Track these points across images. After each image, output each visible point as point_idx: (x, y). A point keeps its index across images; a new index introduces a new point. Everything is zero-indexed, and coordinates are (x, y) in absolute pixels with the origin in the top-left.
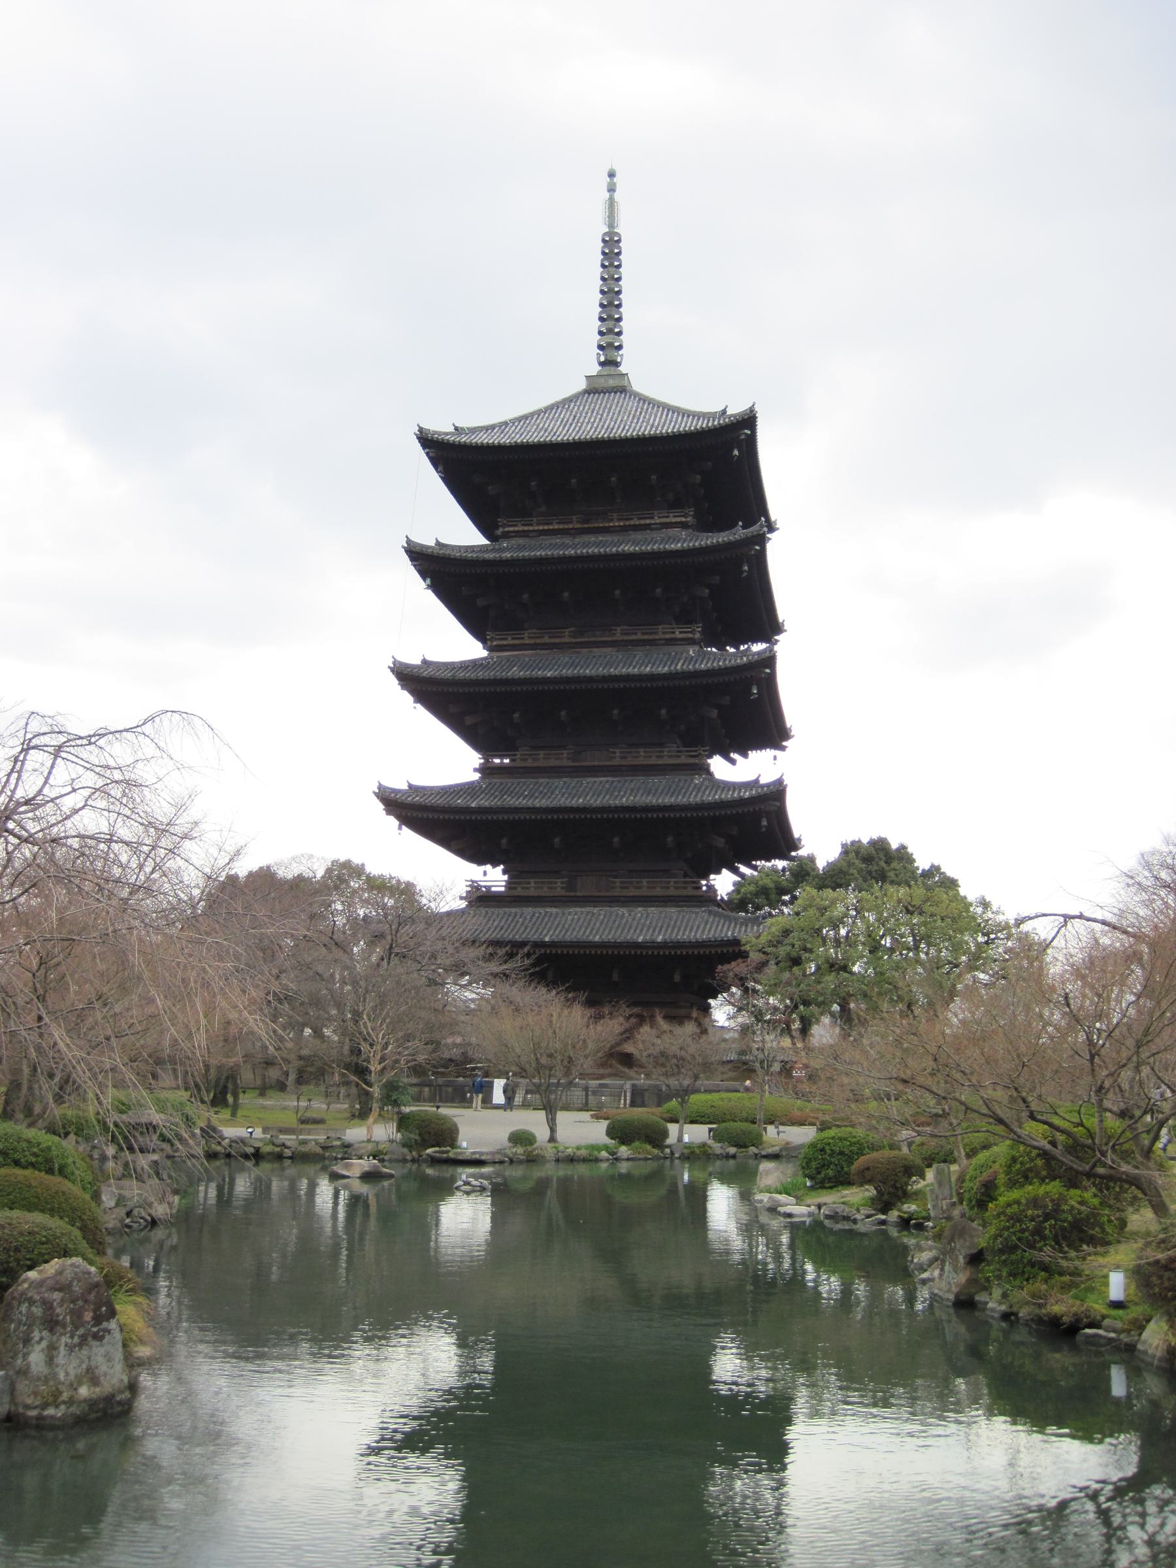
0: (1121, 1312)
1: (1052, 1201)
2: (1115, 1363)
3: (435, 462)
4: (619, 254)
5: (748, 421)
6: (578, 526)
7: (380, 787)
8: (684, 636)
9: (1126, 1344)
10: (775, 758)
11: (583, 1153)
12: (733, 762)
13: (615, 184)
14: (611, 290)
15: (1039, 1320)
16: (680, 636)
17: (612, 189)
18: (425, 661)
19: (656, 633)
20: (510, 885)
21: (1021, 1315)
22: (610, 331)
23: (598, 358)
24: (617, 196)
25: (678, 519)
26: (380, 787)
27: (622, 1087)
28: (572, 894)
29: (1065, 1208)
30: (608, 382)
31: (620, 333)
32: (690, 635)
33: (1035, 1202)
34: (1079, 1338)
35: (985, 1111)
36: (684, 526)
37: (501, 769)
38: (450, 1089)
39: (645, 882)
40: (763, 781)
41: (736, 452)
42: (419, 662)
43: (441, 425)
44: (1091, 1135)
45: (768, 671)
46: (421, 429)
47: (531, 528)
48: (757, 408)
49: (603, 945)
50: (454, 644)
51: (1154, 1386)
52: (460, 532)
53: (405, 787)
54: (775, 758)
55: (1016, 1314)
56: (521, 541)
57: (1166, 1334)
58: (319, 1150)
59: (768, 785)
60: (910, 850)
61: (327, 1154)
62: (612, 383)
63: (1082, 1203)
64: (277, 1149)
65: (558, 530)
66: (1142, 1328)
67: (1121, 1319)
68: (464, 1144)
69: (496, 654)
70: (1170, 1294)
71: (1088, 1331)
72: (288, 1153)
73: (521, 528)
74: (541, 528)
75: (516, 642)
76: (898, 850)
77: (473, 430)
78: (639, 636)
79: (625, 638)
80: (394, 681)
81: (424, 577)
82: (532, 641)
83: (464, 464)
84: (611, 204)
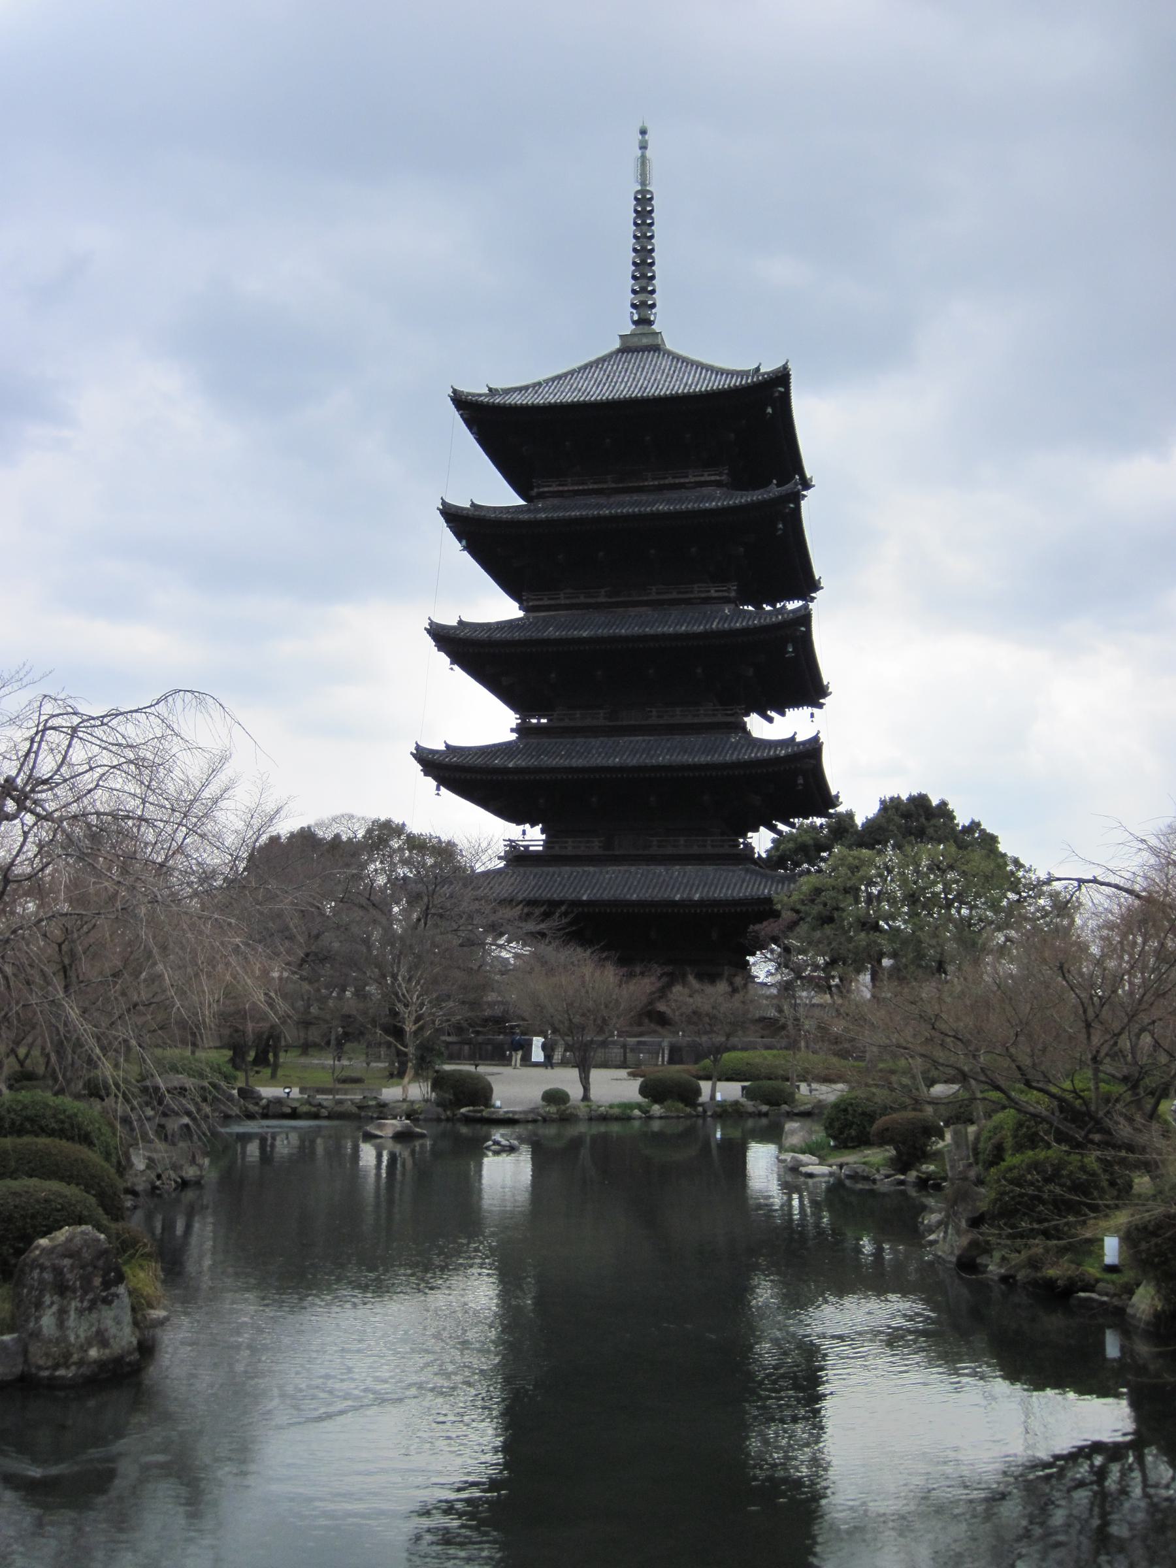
0: (1114, 1276)
1: (1052, 1165)
2: (1110, 1327)
3: (469, 423)
4: (652, 211)
5: (782, 378)
6: (614, 485)
7: (418, 747)
8: (720, 594)
9: (1116, 1307)
10: (812, 715)
11: (616, 1111)
12: (770, 720)
13: (646, 142)
14: (644, 248)
15: (1035, 1283)
16: (716, 595)
17: (643, 147)
18: (461, 622)
20: (547, 843)
21: (1018, 1278)
23: (632, 317)
24: (648, 153)
25: (713, 478)
26: (418, 747)
27: (660, 1044)
28: (610, 853)
29: (1064, 1172)
30: (642, 343)
31: (653, 292)
32: (726, 594)
33: (1035, 1166)
34: (1073, 1302)
35: (983, 1079)
36: (718, 484)
37: (539, 729)
38: (490, 1047)
39: (682, 840)
40: (799, 739)
41: (769, 410)
43: (475, 387)
44: (1086, 1103)
45: (803, 629)
46: (455, 391)
48: (790, 366)
49: (641, 903)
51: (1143, 1349)
52: (496, 492)
53: (443, 747)
54: (812, 715)
55: (1013, 1277)
56: (556, 501)
57: (1153, 1299)
58: (354, 1110)
59: (804, 743)
60: (950, 807)
61: (363, 1114)
62: (645, 341)
63: (1083, 1168)
64: (314, 1109)
66: (1131, 1293)
67: (1113, 1283)
68: (498, 1103)
69: (532, 615)
70: (1156, 1260)
71: (1082, 1294)
72: (324, 1112)
75: (552, 602)
76: (938, 806)
77: (507, 391)
78: (674, 595)
81: (459, 537)
82: (568, 602)
83: (494, 423)
84: (643, 161)
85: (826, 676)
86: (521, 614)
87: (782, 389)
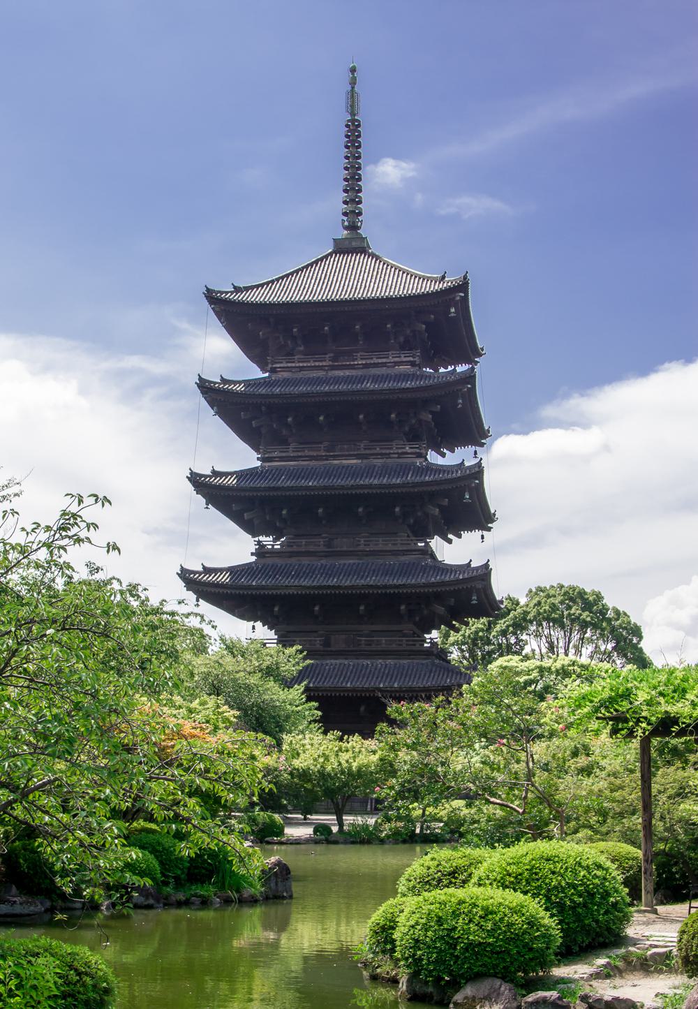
6: (331, 363)
10: (483, 537)
12: (450, 541)
16: (410, 451)
17: (353, 82)
19: (391, 449)
22: (353, 201)
23: (343, 223)
30: (352, 245)
32: (418, 451)
37: (273, 553)
40: (473, 565)
42: (208, 472)
43: (223, 286)
45: (477, 481)
47: (293, 365)
50: (237, 457)
54: (483, 537)
62: (354, 244)
65: (315, 366)
73: (285, 365)
74: (301, 365)
77: (247, 289)
78: (378, 450)
79: (368, 452)
80: (190, 487)
82: (295, 454)
84: (352, 96)
85: (494, 501)
86: (259, 464)
87: (463, 295)
